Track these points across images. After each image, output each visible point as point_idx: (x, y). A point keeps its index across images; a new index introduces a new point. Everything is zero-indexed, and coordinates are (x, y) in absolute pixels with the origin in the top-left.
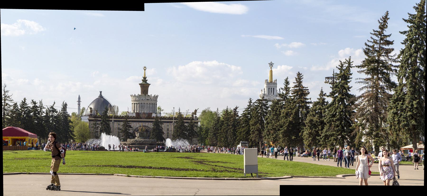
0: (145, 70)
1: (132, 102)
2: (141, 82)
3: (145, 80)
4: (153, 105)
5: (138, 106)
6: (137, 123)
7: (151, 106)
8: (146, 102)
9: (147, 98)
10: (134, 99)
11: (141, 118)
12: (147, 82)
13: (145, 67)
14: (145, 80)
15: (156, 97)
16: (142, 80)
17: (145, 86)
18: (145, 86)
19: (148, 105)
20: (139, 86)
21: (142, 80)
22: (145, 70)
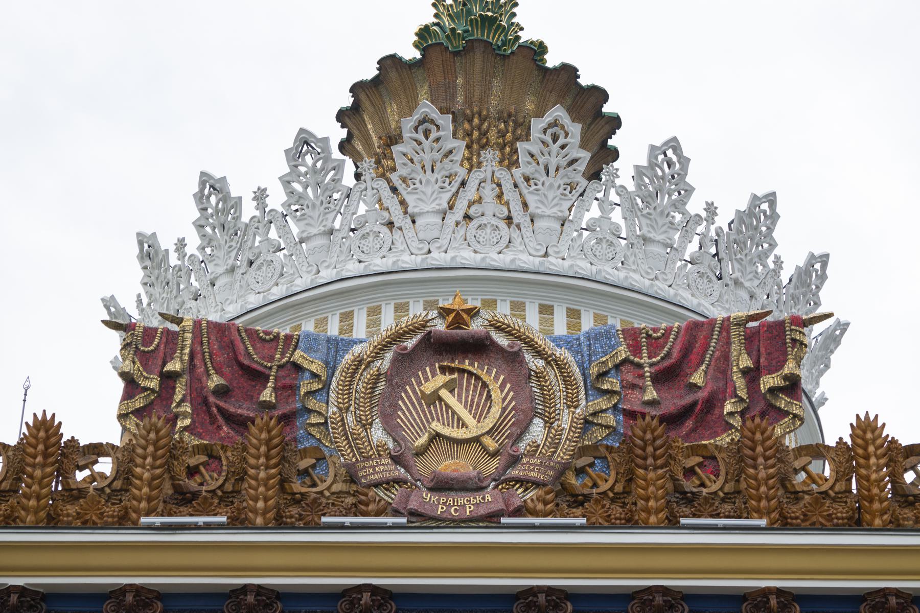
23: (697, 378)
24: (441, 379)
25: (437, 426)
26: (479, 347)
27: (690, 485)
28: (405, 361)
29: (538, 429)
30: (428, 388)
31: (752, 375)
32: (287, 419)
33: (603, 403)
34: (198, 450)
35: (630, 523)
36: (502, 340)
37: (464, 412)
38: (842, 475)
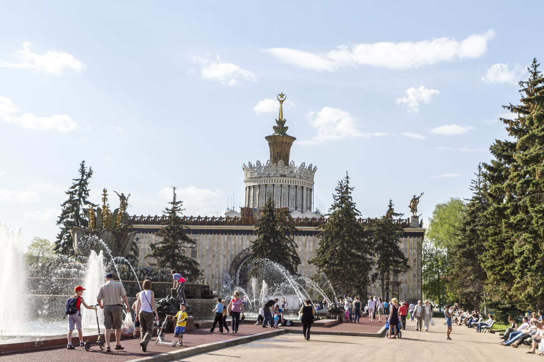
0: (281, 102)
1: (245, 185)
2: (272, 132)
3: (281, 126)
4: (299, 191)
5: (257, 193)
6: (245, 237)
7: (292, 192)
8: (278, 181)
9: (281, 172)
10: (249, 176)
12: (288, 133)
13: (282, 95)
14: (281, 126)
15: (309, 172)
16: (274, 127)
17: (280, 142)
18: (280, 142)
19: (285, 191)
20: (267, 142)
21: (274, 127)
22: (281, 102)
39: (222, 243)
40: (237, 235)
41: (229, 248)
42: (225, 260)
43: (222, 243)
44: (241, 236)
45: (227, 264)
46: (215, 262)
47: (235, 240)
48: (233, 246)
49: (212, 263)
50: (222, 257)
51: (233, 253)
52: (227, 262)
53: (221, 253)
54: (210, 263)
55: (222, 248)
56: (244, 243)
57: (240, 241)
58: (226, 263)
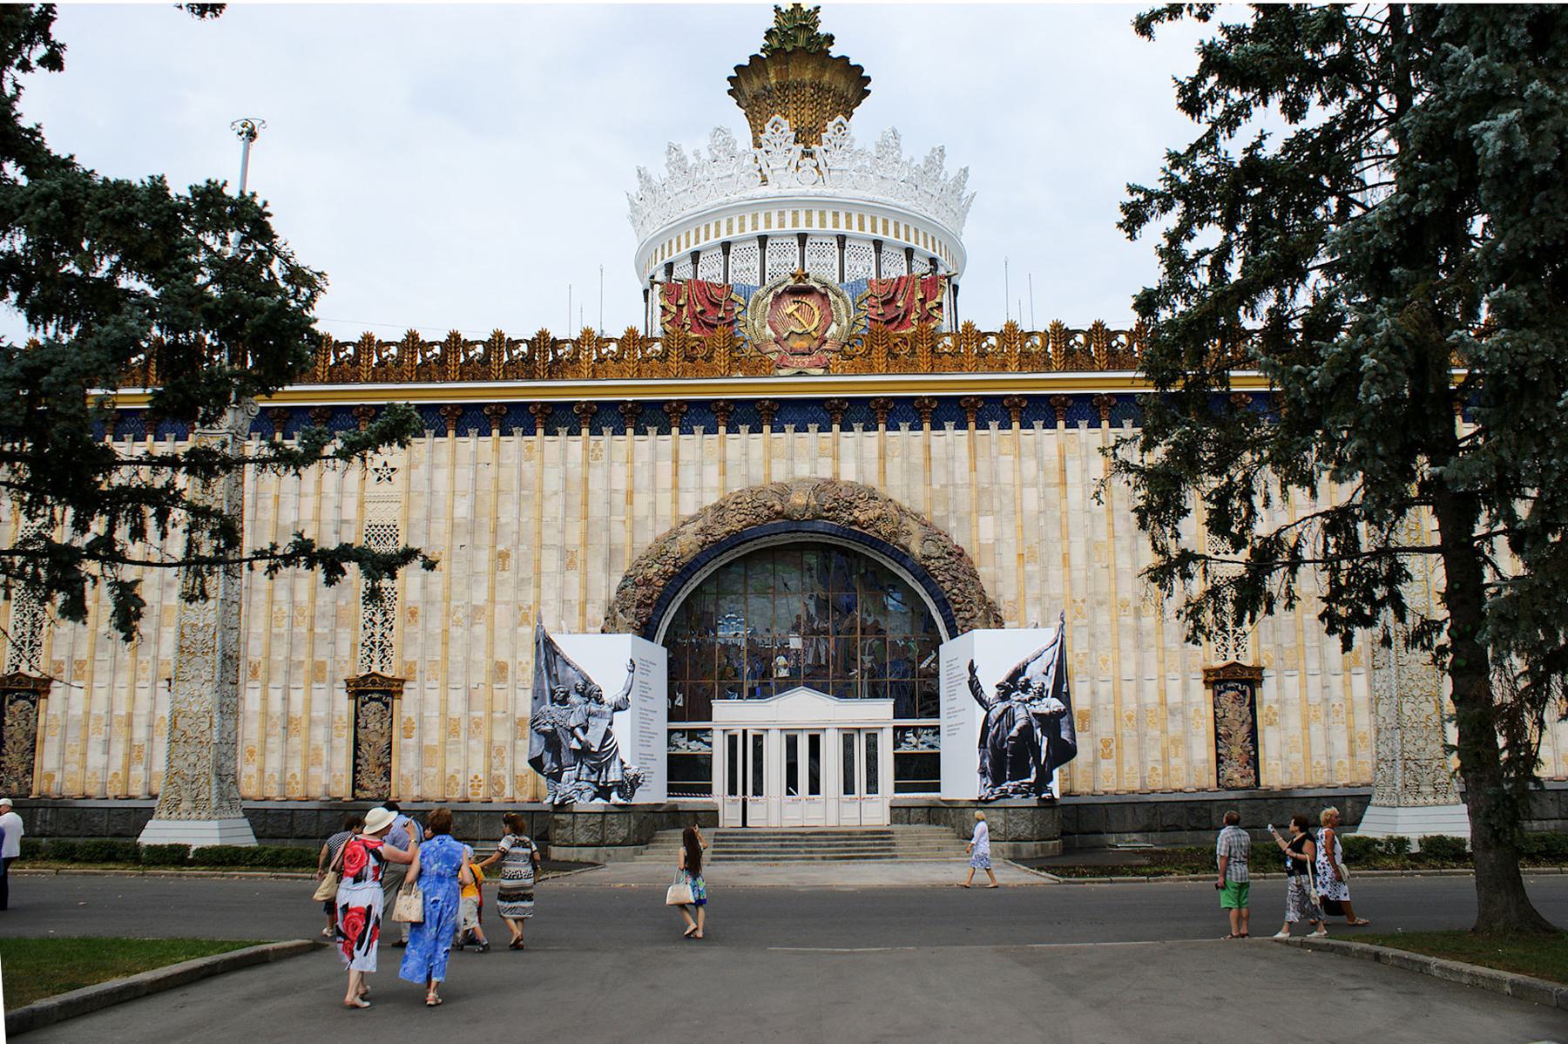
6: (695, 446)
11: (758, 365)
23: (900, 304)
24: (795, 307)
25: (792, 328)
26: (810, 291)
27: (896, 351)
28: (778, 297)
29: (834, 328)
30: (789, 311)
31: (923, 301)
32: (731, 324)
33: (861, 314)
34: (697, 339)
35: (871, 370)
36: (818, 286)
37: (801, 317)
38: (957, 346)
39: (553, 480)
40: (641, 431)
41: (597, 510)
42: (574, 579)
43: (553, 480)
44: (666, 443)
45: (584, 604)
46: (505, 594)
47: (630, 460)
48: (620, 499)
49: (492, 600)
50: (551, 562)
51: (621, 536)
52: (585, 588)
53: (551, 536)
54: (480, 596)
55: (554, 508)
56: (688, 477)
57: (666, 466)
58: (575, 595)
